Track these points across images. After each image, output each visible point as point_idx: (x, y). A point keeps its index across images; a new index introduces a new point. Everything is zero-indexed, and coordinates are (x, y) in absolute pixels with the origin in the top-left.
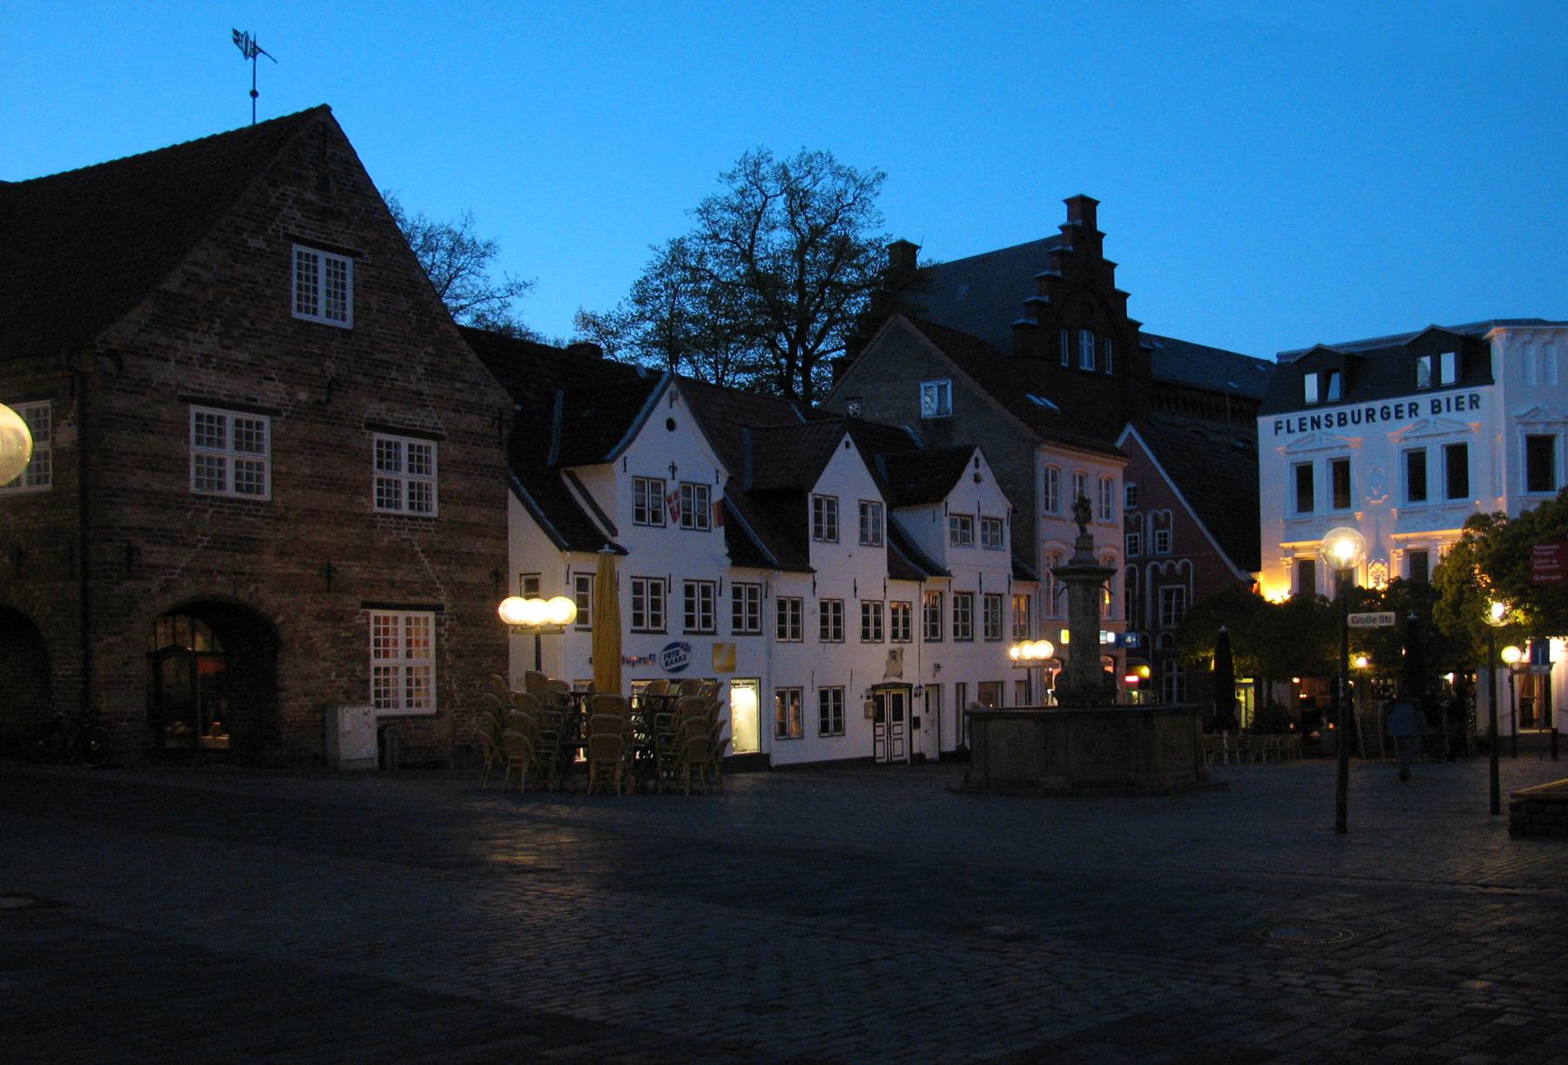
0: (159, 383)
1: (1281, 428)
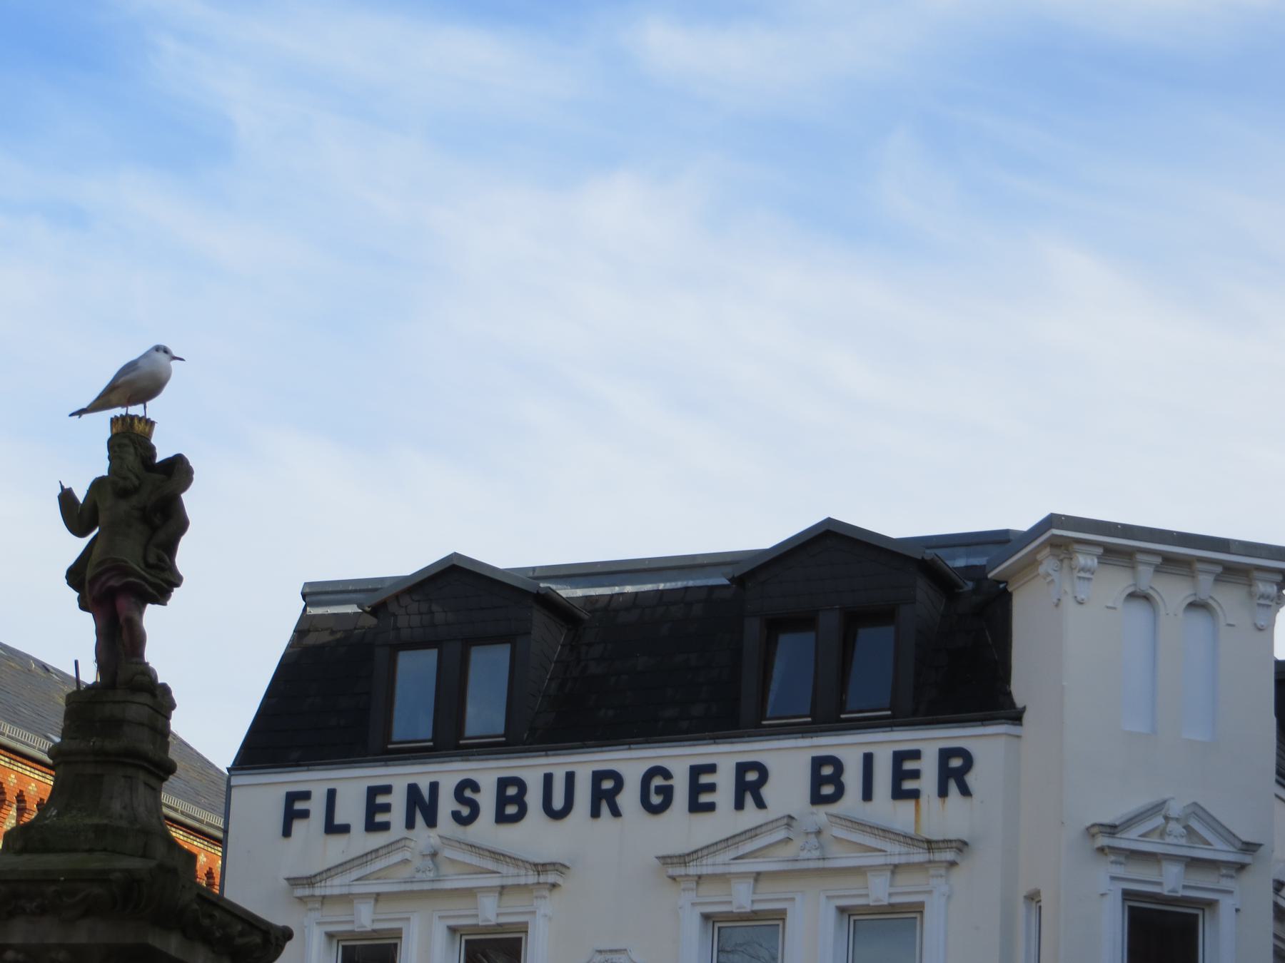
1: (305, 814)
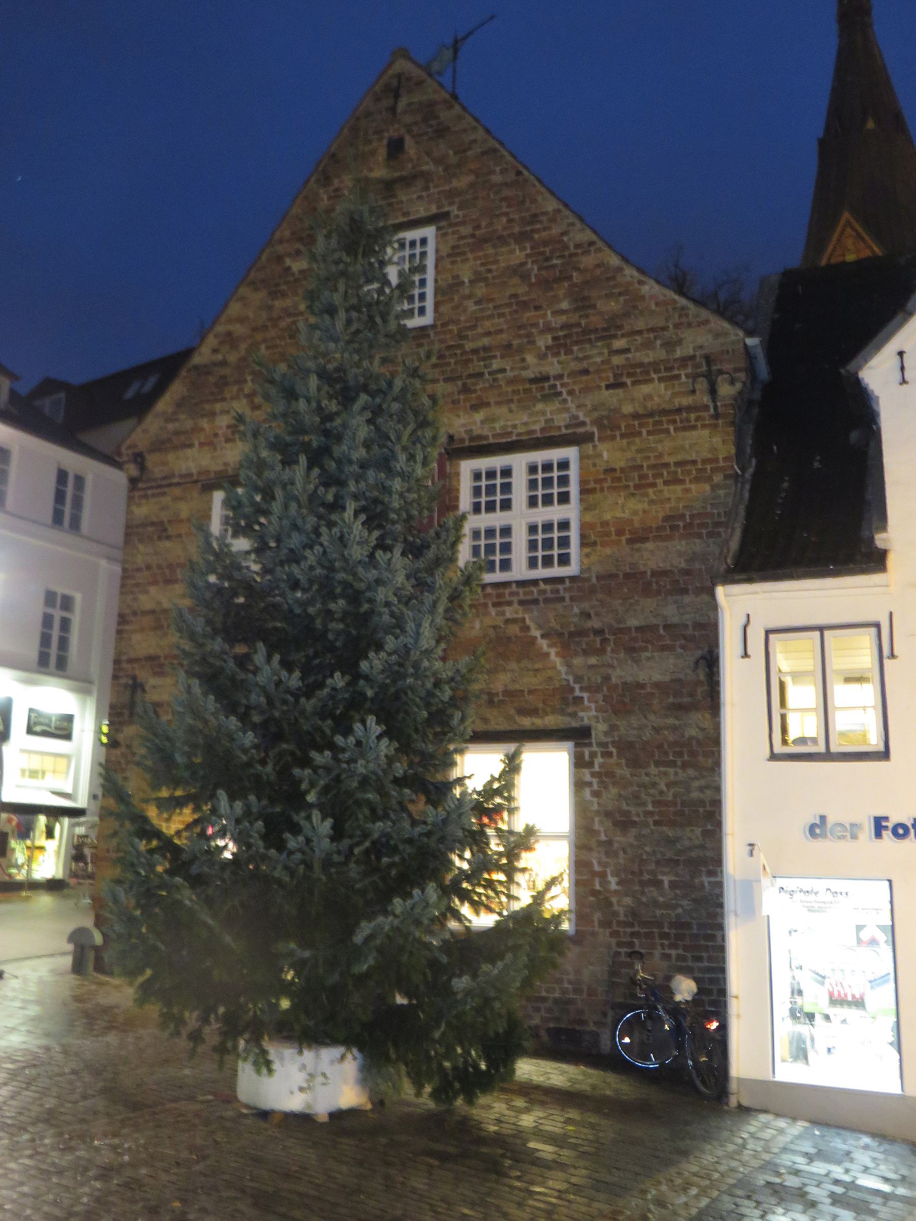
0: (181, 476)
